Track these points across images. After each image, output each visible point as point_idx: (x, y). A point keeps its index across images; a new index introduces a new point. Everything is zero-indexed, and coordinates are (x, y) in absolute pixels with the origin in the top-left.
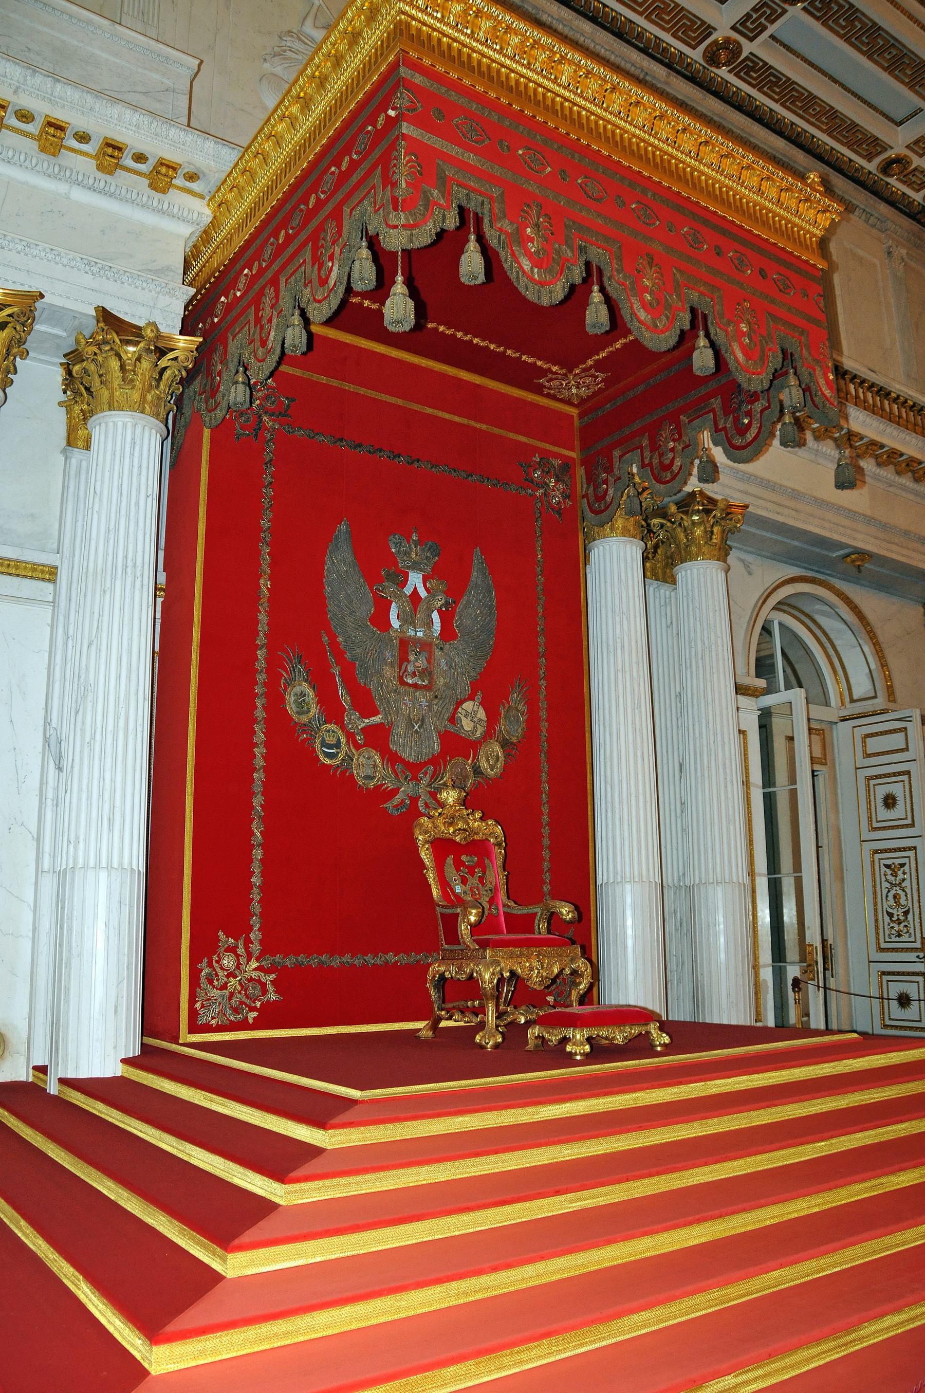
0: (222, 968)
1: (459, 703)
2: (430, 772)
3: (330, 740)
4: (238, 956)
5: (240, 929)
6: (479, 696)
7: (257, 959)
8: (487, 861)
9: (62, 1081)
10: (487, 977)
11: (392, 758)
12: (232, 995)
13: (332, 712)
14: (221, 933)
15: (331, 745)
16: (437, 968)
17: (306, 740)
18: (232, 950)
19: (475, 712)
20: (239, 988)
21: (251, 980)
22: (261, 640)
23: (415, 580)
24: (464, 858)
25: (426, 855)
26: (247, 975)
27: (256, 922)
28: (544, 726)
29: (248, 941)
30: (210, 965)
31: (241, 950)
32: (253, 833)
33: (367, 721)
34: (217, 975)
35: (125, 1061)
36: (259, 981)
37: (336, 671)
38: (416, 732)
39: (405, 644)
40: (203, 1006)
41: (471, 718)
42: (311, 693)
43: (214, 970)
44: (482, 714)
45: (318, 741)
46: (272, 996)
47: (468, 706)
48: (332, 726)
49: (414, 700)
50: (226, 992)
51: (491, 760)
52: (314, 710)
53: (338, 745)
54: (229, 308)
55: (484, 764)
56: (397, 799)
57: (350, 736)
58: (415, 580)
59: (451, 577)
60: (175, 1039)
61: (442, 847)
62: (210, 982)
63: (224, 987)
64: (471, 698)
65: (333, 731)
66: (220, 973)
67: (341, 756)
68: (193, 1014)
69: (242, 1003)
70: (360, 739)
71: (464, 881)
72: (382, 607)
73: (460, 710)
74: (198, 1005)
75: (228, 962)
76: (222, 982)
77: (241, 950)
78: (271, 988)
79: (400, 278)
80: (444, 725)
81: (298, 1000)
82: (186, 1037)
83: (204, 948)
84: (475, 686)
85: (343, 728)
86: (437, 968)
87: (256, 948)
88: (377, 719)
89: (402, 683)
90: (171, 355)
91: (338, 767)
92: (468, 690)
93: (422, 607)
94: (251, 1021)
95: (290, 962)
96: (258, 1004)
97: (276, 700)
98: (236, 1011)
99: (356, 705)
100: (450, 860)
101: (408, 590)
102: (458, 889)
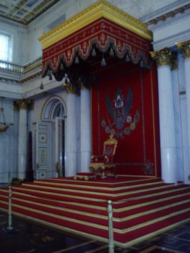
13: (107, 124)
15: (107, 129)
23: (119, 97)
25: (104, 147)
41: (129, 118)
44: (131, 118)
47: (128, 117)
51: (133, 126)
52: (105, 124)
55: (131, 128)
57: (110, 127)
59: (124, 94)
61: (107, 146)
64: (129, 115)
80: (124, 121)
101: (118, 99)
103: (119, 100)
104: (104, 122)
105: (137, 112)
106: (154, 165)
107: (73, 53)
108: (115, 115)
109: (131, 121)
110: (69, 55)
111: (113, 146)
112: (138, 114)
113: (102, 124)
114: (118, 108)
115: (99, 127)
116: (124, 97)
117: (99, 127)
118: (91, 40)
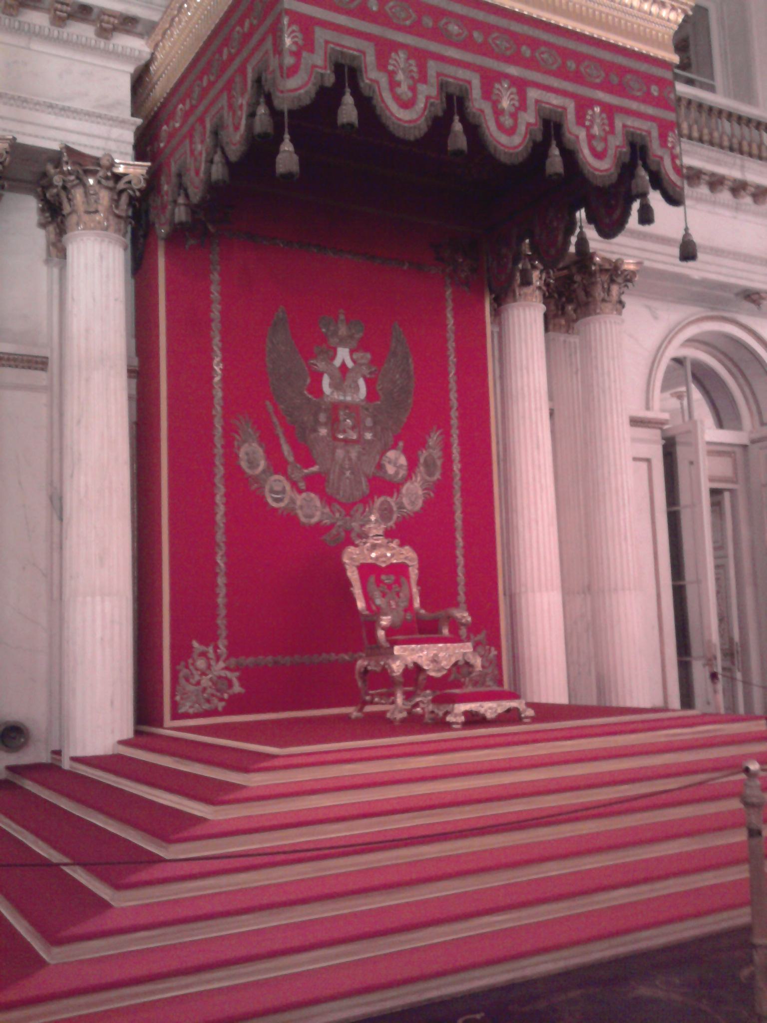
0: (197, 669)
1: (383, 453)
2: (361, 510)
3: (278, 488)
4: (208, 659)
5: (209, 637)
6: (401, 444)
7: (225, 661)
8: (403, 580)
9: (75, 759)
10: (397, 667)
11: (329, 500)
12: (204, 689)
13: (278, 465)
14: (195, 644)
15: (280, 493)
16: (361, 664)
17: (258, 489)
18: (204, 654)
19: (397, 459)
20: (210, 684)
21: (220, 677)
22: (218, 410)
23: (343, 355)
24: (383, 577)
25: (353, 575)
26: (216, 673)
27: (223, 632)
28: (457, 467)
29: (216, 648)
30: (187, 667)
31: (211, 654)
32: (216, 564)
33: (306, 471)
34: (192, 674)
35: (123, 743)
36: (226, 678)
37: (279, 431)
38: (348, 478)
39: (335, 407)
40: (182, 699)
41: (395, 462)
42: (260, 452)
43: (190, 670)
44: (403, 461)
45: (267, 488)
46: (237, 688)
47: (391, 454)
48: (277, 477)
49: (348, 452)
50: (200, 688)
51: (413, 496)
52: (262, 464)
53: (284, 491)
54: (171, 136)
55: (405, 501)
56: (334, 531)
57: (294, 484)
58: (343, 355)
60: (161, 725)
61: (367, 570)
62: (187, 680)
63: (198, 683)
64: (394, 447)
65: (280, 481)
66: (194, 672)
67: (286, 501)
68: (175, 705)
69: (213, 695)
70: (302, 485)
71: (384, 595)
72: (317, 377)
73: (384, 458)
74: (178, 698)
75: (201, 663)
76: (197, 678)
77: (211, 654)
78: (236, 683)
79: (287, 137)
80: (370, 470)
81: (258, 692)
82: (167, 721)
83: (181, 653)
84: (397, 438)
85: (288, 478)
86: (361, 664)
87: (223, 650)
88: (315, 469)
89: (335, 439)
90: (126, 179)
91: (285, 508)
92: (391, 441)
93: (349, 375)
94: (220, 709)
95: (250, 661)
96: (226, 696)
97: (231, 458)
98: (208, 701)
99: (298, 459)
100: (372, 579)
101: (337, 363)
102: (379, 601)
103: (343, 366)
104: (251, 454)
105: (434, 438)
106: (499, 657)
107: (529, 117)
108: (323, 431)
109: (403, 473)
110: (505, 104)
111: (400, 570)
112: (437, 453)
113: (242, 454)
114: (347, 406)
115: (220, 471)
116: (372, 362)
117: (220, 471)
118: (631, 122)
